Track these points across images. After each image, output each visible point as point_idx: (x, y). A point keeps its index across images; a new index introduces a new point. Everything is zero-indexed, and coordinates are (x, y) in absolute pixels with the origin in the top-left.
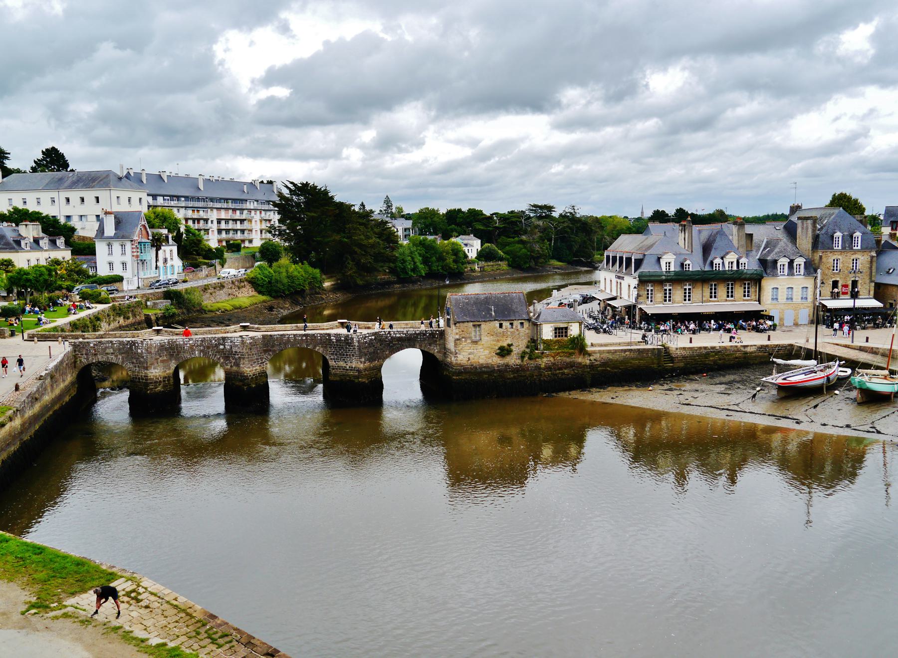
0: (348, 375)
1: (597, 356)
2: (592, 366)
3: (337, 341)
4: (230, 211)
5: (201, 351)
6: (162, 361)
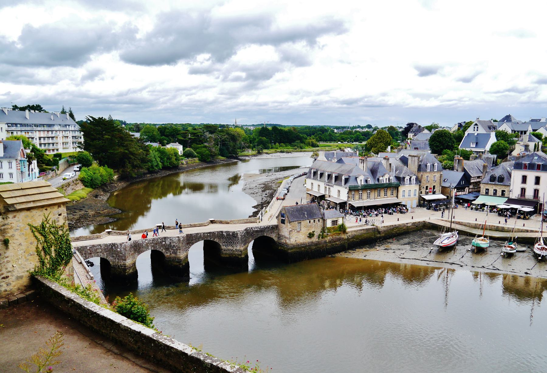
1: (350, 234)
2: (348, 239)
4: (46, 132)
6: (132, 254)
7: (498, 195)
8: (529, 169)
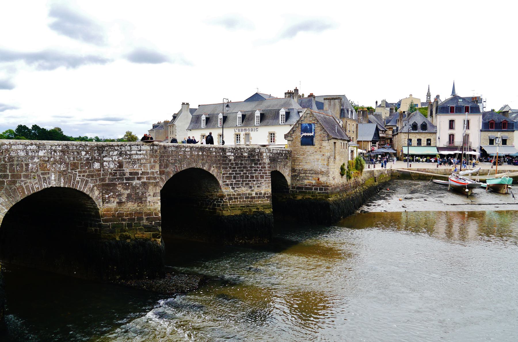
0: (255, 206)
3: (236, 158)
5: (62, 174)
7: (422, 145)
8: (456, 112)
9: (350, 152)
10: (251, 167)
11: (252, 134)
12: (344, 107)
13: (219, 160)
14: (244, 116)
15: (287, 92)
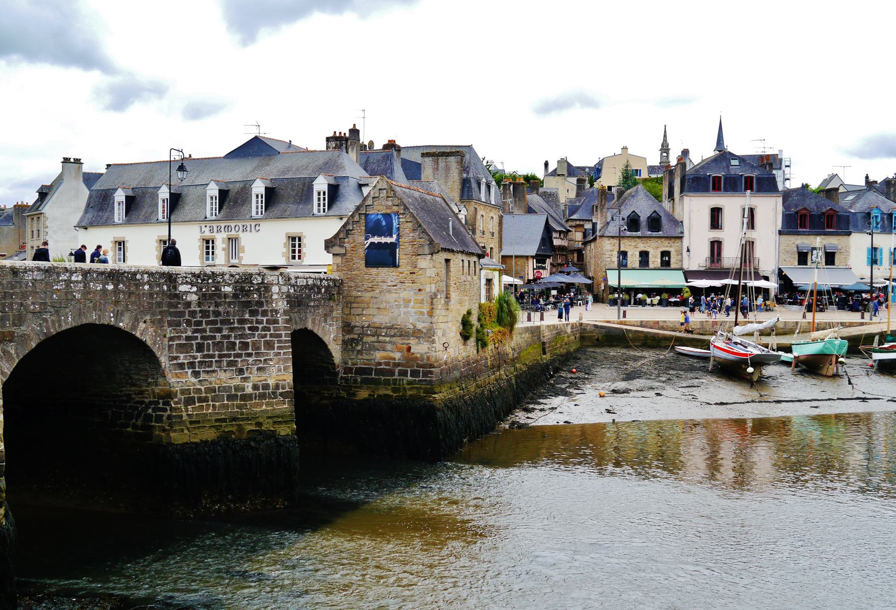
3: (204, 298)
7: (651, 266)
8: (726, 190)
9: (483, 282)
10: (242, 321)
11: (246, 239)
12: (471, 175)
13: (159, 304)
14: (223, 195)
15: (331, 135)
